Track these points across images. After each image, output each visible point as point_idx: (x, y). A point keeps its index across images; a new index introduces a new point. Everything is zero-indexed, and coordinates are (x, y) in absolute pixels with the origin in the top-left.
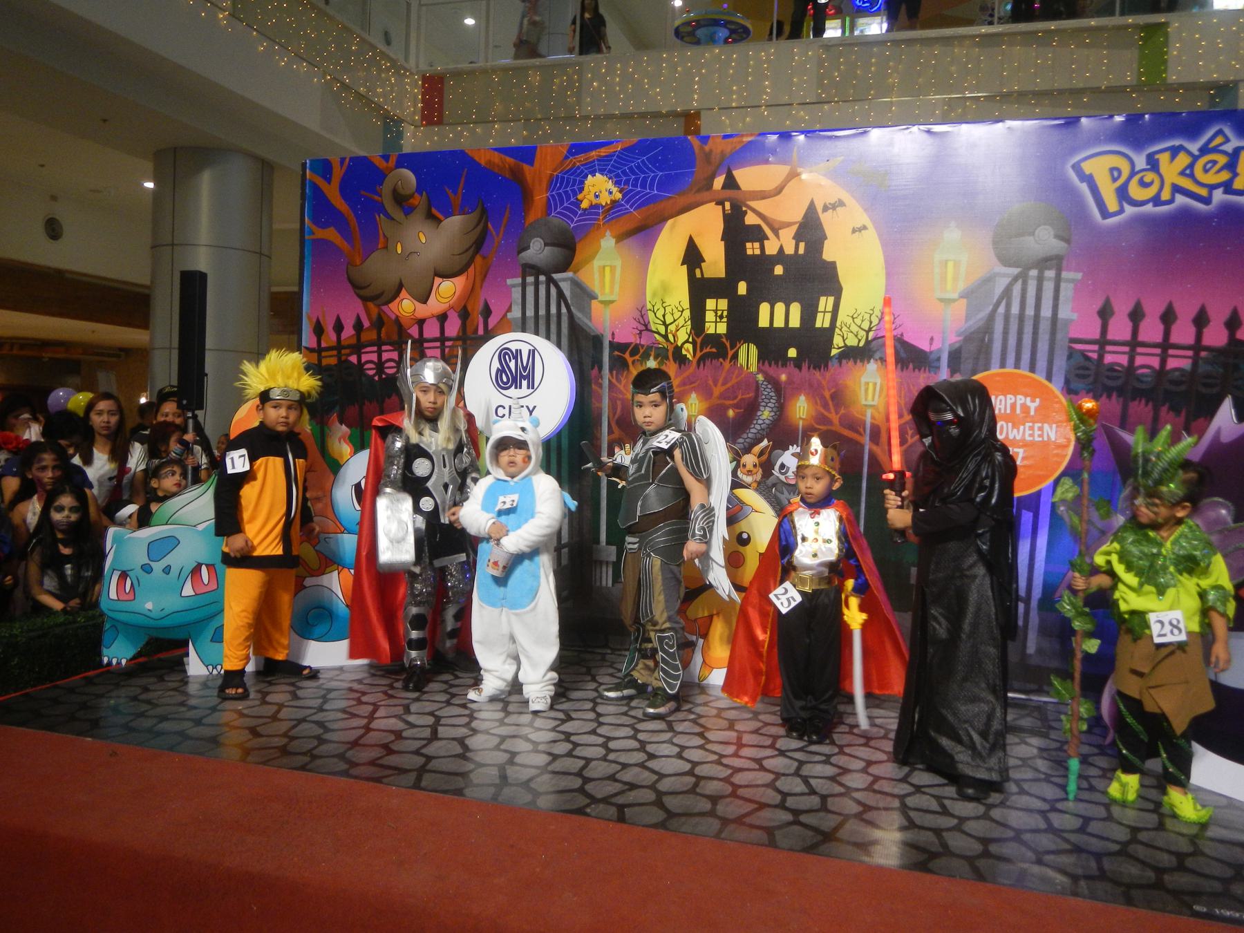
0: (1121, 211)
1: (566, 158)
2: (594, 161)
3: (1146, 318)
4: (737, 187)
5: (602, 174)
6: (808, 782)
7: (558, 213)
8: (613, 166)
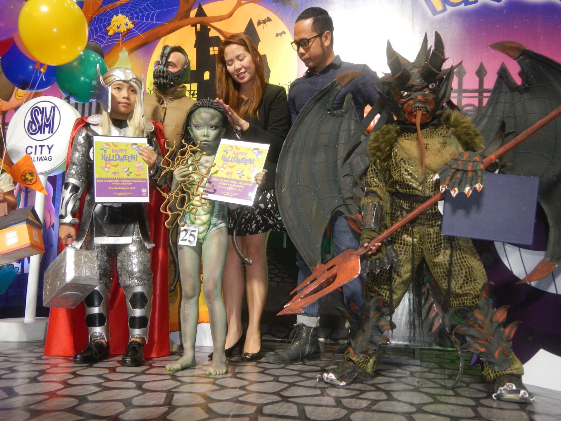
0: (445, 10)
1: (101, 6)
2: (118, 7)
3: (466, 74)
4: (205, 15)
5: (122, 14)
6: (173, 396)
7: (95, 39)
8: (128, 9)
